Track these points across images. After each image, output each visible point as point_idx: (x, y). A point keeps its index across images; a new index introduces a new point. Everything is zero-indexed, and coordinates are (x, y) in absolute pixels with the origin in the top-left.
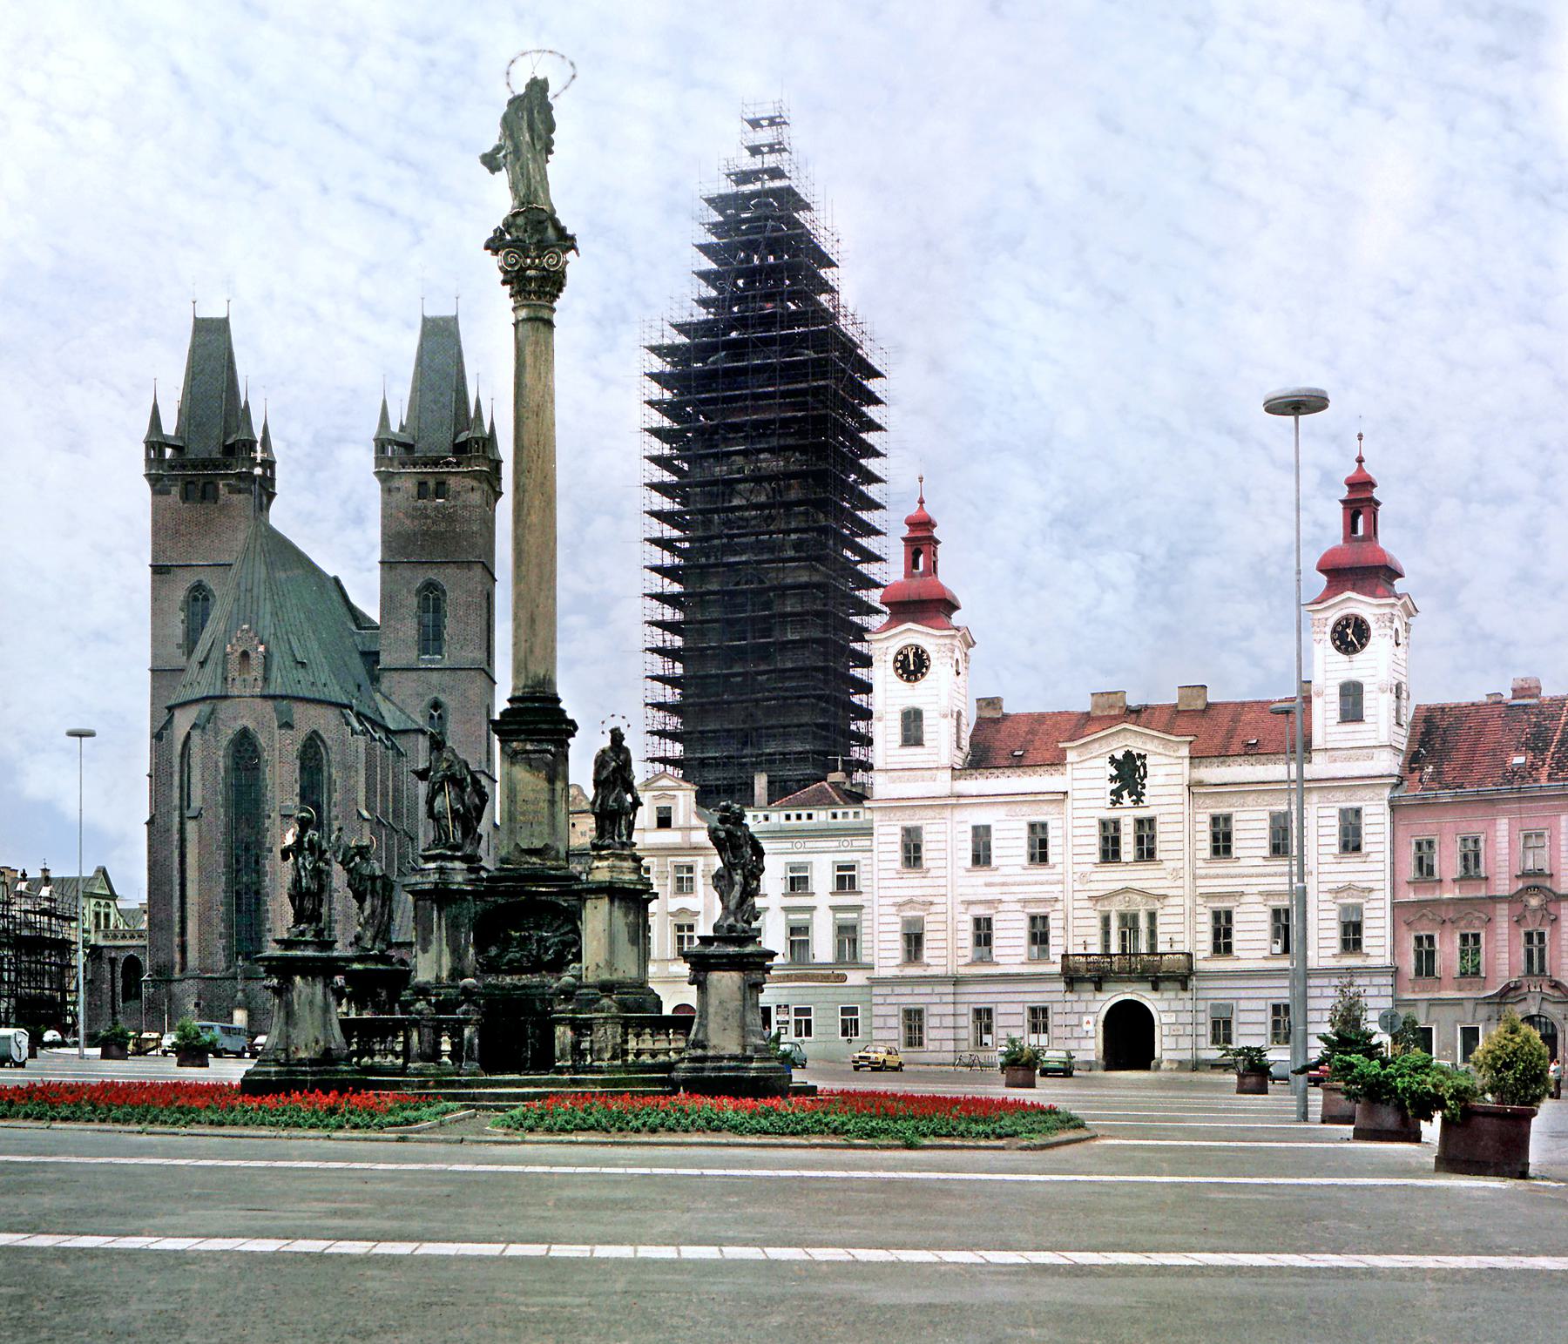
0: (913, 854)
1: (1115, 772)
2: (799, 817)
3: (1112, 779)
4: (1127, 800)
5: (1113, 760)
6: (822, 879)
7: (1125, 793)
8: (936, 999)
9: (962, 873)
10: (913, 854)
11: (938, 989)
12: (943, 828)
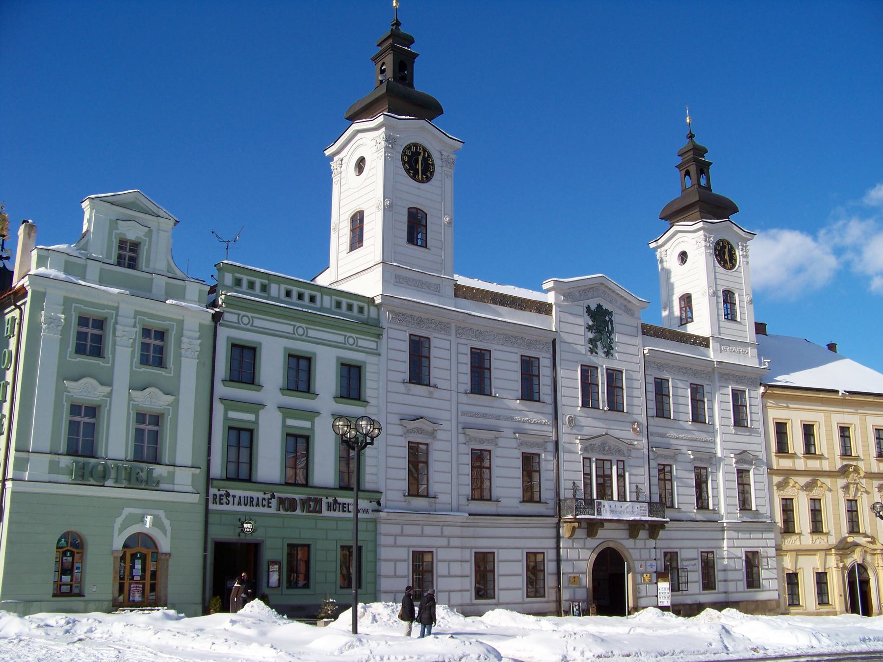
0: (419, 370)
1: (591, 323)
2: (300, 296)
3: (589, 328)
4: (601, 352)
5: (588, 308)
6: (326, 378)
7: (599, 343)
8: (443, 542)
9: (464, 398)
10: (419, 370)
11: (448, 531)
12: (446, 344)
